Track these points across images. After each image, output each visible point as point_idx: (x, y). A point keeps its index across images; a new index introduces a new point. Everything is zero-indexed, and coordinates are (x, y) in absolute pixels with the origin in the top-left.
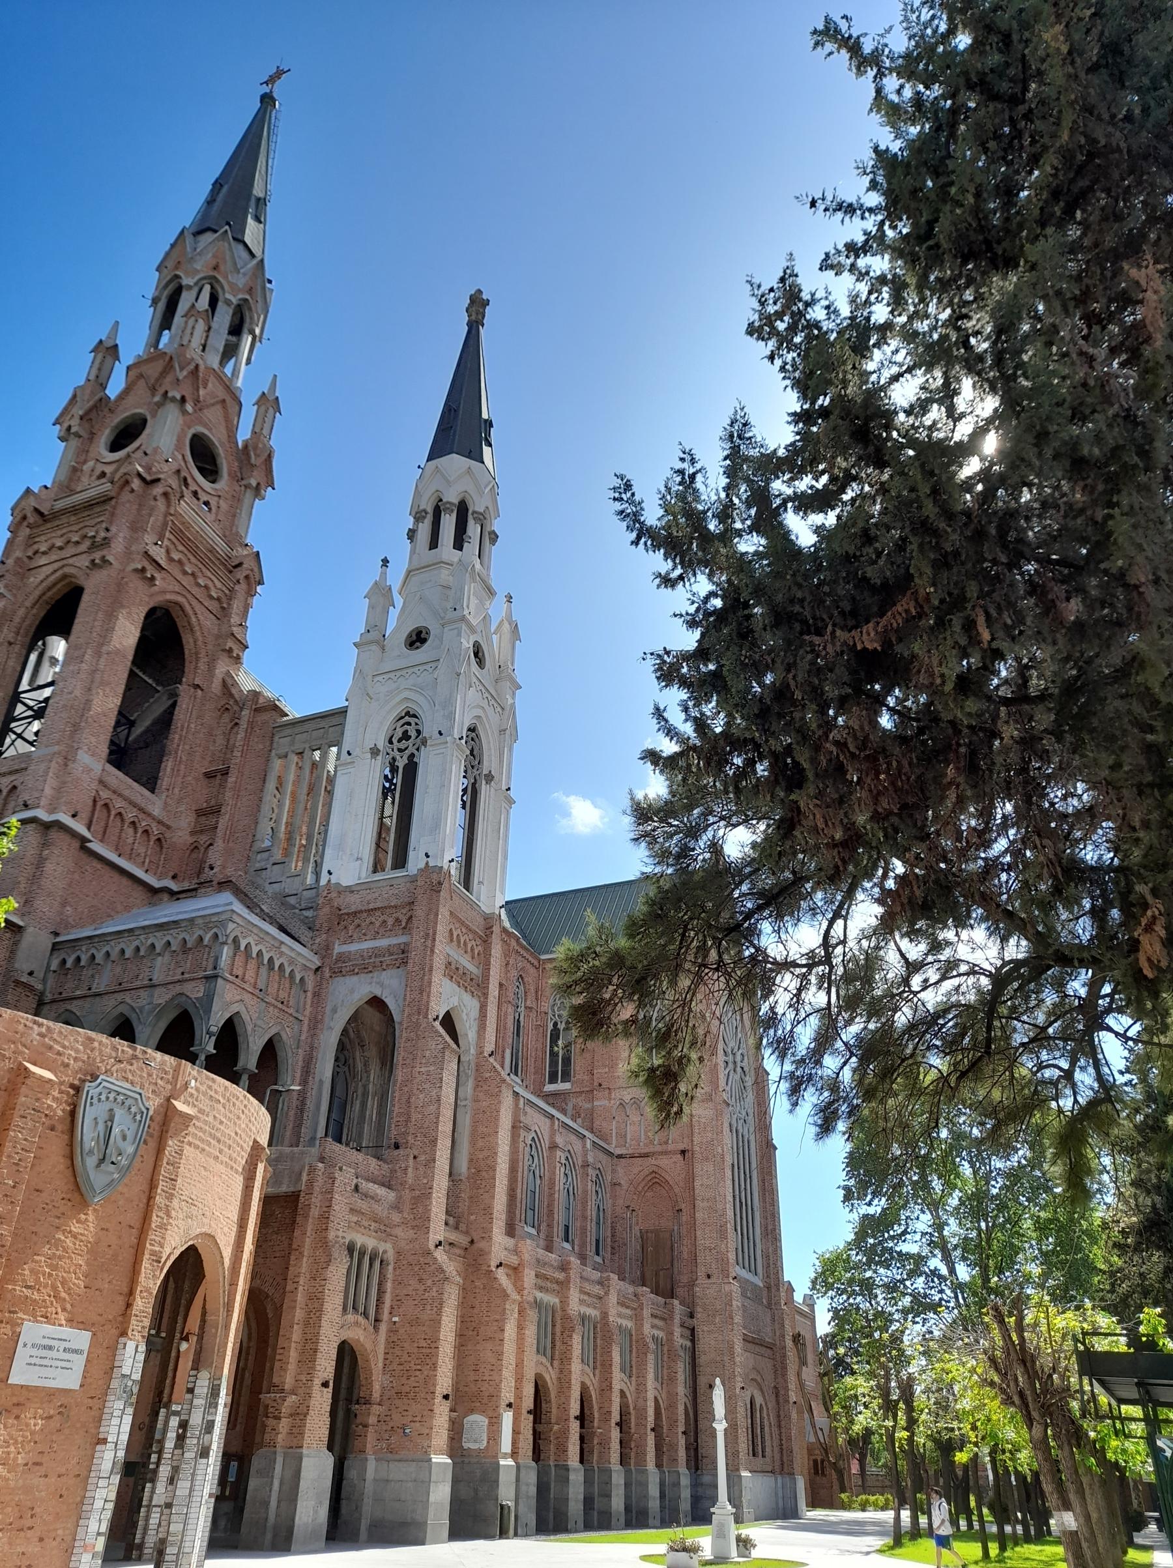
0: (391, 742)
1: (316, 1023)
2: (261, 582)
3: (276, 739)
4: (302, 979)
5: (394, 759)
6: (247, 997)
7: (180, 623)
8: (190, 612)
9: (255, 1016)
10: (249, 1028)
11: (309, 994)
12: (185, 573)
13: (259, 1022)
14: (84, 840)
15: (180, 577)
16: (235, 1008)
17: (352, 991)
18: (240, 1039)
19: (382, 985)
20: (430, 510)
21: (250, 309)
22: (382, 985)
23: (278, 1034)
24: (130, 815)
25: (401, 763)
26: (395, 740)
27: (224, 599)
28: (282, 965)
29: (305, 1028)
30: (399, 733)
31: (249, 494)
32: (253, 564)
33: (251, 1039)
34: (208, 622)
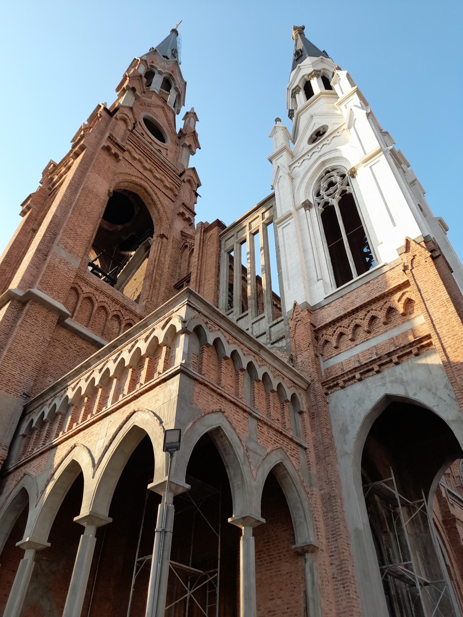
0: (318, 195)
1: (325, 452)
2: (199, 185)
3: (223, 242)
4: (294, 396)
5: (327, 203)
6: (229, 409)
7: (147, 201)
8: (152, 193)
9: (244, 437)
10: (240, 452)
11: (306, 416)
12: (145, 168)
13: (252, 445)
14: (62, 316)
15: (141, 170)
16: (213, 421)
17: (360, 401)
18: (230, 472)
19: (402, 382)
20: (302, 86)
21: (173, 80)
22: (402, 382)
23: (279, 466)
24: (112, 308)
25: (334, 202)
26: (322, 192)
27: (175, 190)
28: (265, 375)
29: (313, 458)
30: (324, 185)
31: (185, 151)
32: (192, 174)
33: (245, 469)
34: (166, 202)
